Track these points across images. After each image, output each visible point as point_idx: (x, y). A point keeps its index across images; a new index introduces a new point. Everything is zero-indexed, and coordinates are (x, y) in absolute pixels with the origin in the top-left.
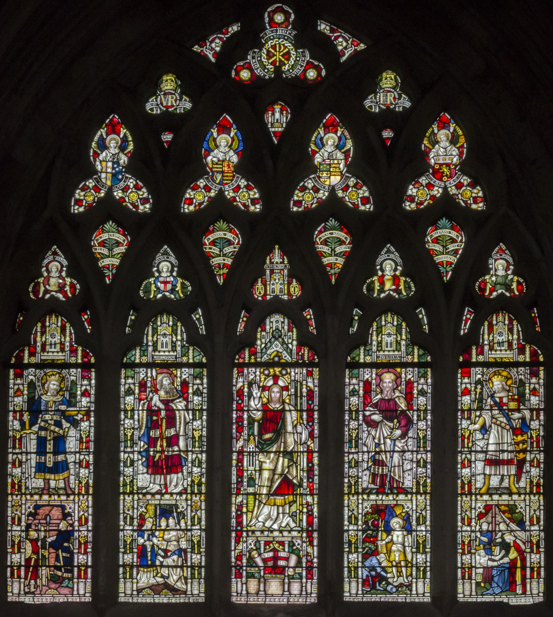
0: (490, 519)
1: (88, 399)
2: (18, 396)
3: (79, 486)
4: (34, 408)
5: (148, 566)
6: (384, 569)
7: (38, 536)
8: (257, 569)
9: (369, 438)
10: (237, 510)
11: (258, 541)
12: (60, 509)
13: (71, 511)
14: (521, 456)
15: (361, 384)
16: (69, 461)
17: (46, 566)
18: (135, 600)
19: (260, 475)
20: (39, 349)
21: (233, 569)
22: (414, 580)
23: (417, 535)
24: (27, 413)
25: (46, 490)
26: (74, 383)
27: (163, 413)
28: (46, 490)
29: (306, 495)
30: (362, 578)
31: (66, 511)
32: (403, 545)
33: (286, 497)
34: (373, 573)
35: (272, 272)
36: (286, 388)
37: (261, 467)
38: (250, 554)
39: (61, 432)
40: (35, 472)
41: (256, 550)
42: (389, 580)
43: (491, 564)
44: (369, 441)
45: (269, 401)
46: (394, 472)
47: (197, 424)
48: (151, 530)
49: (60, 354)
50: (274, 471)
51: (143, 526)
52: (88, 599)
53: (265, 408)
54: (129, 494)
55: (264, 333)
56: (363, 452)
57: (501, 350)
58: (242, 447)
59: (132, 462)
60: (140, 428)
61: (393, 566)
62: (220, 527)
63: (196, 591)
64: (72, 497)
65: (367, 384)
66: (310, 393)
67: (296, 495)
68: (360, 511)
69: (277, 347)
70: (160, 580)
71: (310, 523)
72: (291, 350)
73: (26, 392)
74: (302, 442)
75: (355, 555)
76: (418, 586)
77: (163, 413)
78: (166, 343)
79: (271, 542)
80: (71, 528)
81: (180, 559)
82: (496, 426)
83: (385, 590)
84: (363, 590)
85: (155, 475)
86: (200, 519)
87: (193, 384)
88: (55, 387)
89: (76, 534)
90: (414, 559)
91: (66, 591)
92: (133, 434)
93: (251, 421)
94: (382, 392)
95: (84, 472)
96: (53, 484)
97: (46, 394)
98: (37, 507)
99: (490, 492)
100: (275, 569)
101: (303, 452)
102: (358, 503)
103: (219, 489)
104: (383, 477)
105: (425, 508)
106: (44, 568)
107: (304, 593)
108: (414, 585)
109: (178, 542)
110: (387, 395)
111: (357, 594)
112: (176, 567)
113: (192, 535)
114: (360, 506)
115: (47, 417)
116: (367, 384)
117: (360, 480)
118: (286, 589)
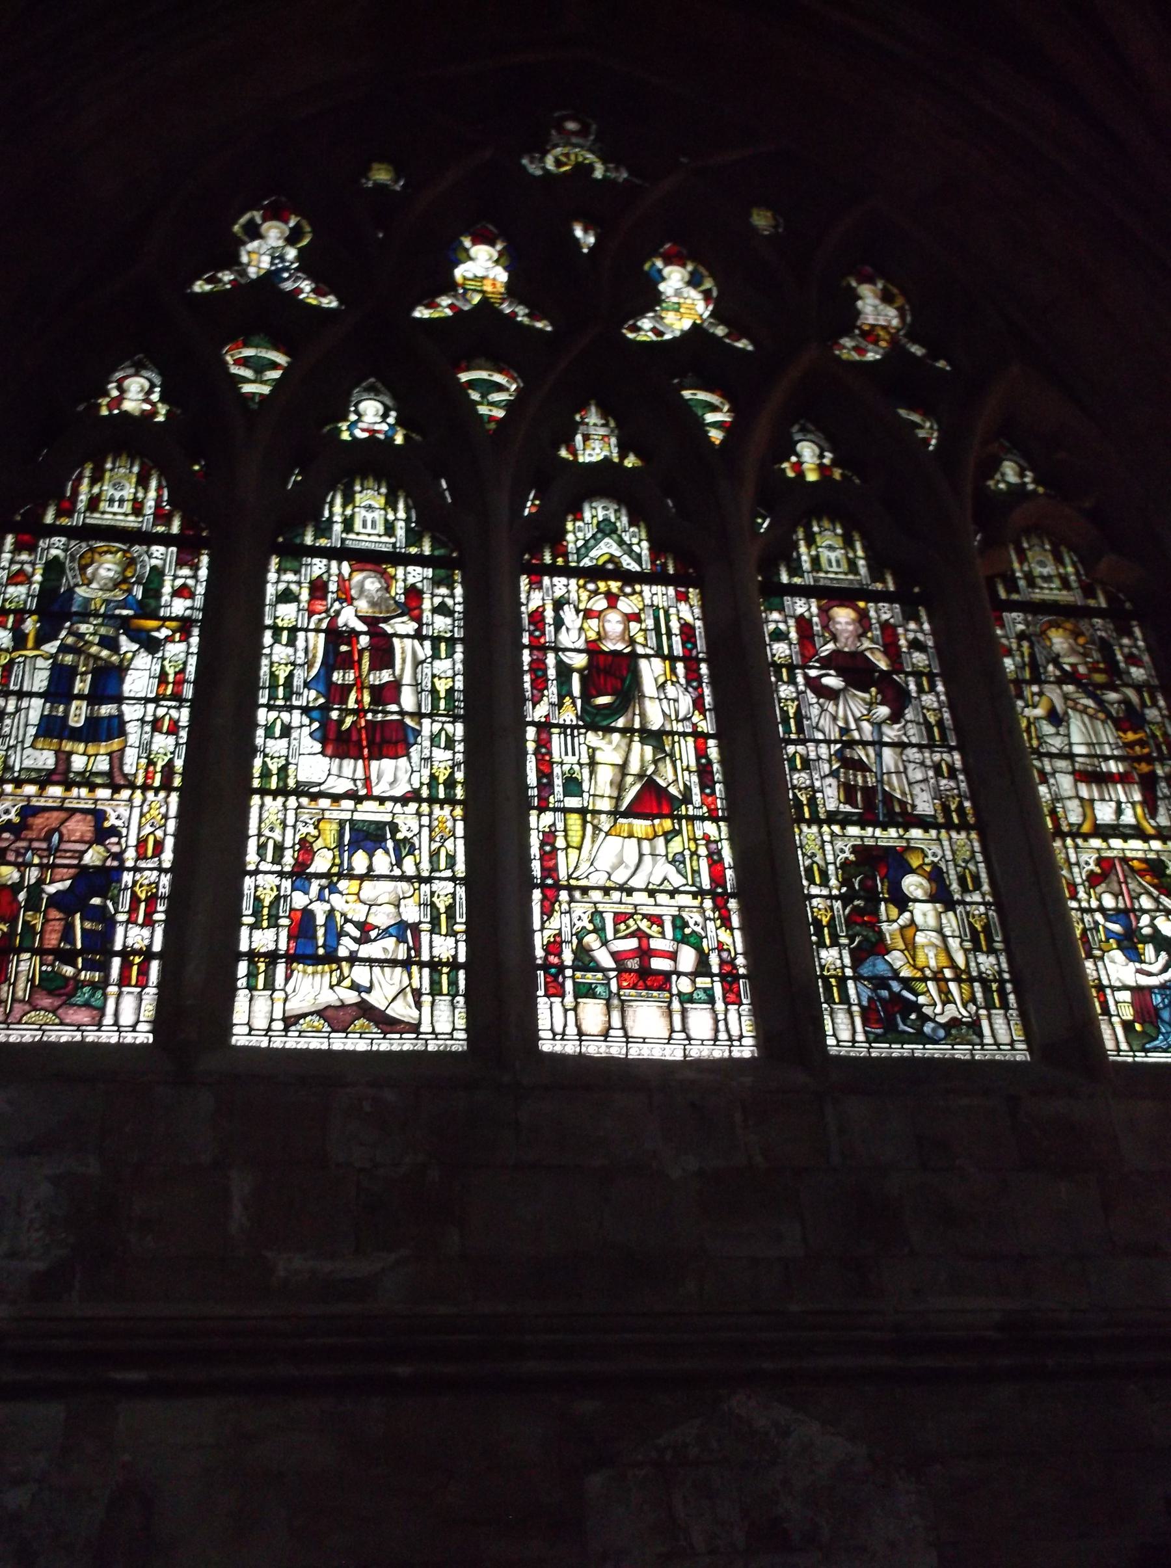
0: (1116, 888)
1: (188, 603)
2: (16, 584)
3: (146, 771)
4: (56, 608)
5: (316, 960)
6: (906, 983)
7: (22, 877)
8: (600, 975)
9: (825, 720)
10: (543, 844)
11: (597, 914)
12: (89, 817)
13: (118, 823)
14: (1144, 768)
15: (791, 622)
16: (127, 718)
17: (34, 952)
18: (277, 1043)
19: (592, 773)
20: (81, 506)
21: (541, 973)
22: (983, 1012)
23: (968, 913)
24: (35, 617)
25: (61, 774)
26: (158, 573)
27: (364, 641)
28: (61, 774)
29: (702, 819)
30: (859, 1004)
31: (107, 824)
32: (940, 931)
33: (657, 821)
34: (885, 993)
35: (586, 438)
36: (636, 617)
37: (592, 757)
38: (580, 941)
39: (115, 658)
40: (36, 736)
41: (595, 931)
42: (927, 1011)
43: (1144, 981)
44: (825, 722)
45: (601, 637)
46: (890, 784)
47: (443, 666)
48: (327, 875)
49: (131, 518)
50: (623, 768)
51: (309, 866)
52: (144, 1036)
53: (592, 649)
54: (275, 794)
55: (579, 524)
56: (818, 742)
57: (1051, 589)
58: (547, 716)
59: (286, 731)
60: (310, 664)
61: (925, 979)
62: (500, 881)
63: (445, 1023)
64: (125, 794)
65: (803, 623)
66: (687, 631)
67: (680, 818)
68: (830, 858)
69: (608, 547)
70: (351, 997)
71: (717, 878)
72: (639, 555)
73: (38, 578)
74: (680, 717)
75: (834, 952)
76: (996, 1026)
77: (364, 641)
78: (374, 523)
79: (631, 916)
80: (115, 863)
81: (403, 948)
82: (1078, 715)
83: (920, 1032)
84: (866, 1032)
85: (342, 758)
86: (451, 860)
87: (433, 595)
88: (111, 574)
89: (127, 878)
90: (973, 964)
91: (83, 1016)
92: (290, 676)
93: (564, 671)
94: (834, 638)
95: (163, 743)
96: (78, 763)
97: (88, 585)
98: (28, 811)
99: (1104, 832)
100: (645, 977)
101: (684, 734)
102: (823, 842)
103: (495, 798)
104: (869, 792)
105: (973, 857)
106: (26, 956)
107: (723, 1036)
108: (985, 1024)
109: (398, 906)
110: (847, 645)
111: (854, 1041)
112: (394, 963)
113: (432, 893)
114: (828, 847)
115: (83, 628)
116: (803, 623)
117: (819, 795)
118: (678, 1025)
